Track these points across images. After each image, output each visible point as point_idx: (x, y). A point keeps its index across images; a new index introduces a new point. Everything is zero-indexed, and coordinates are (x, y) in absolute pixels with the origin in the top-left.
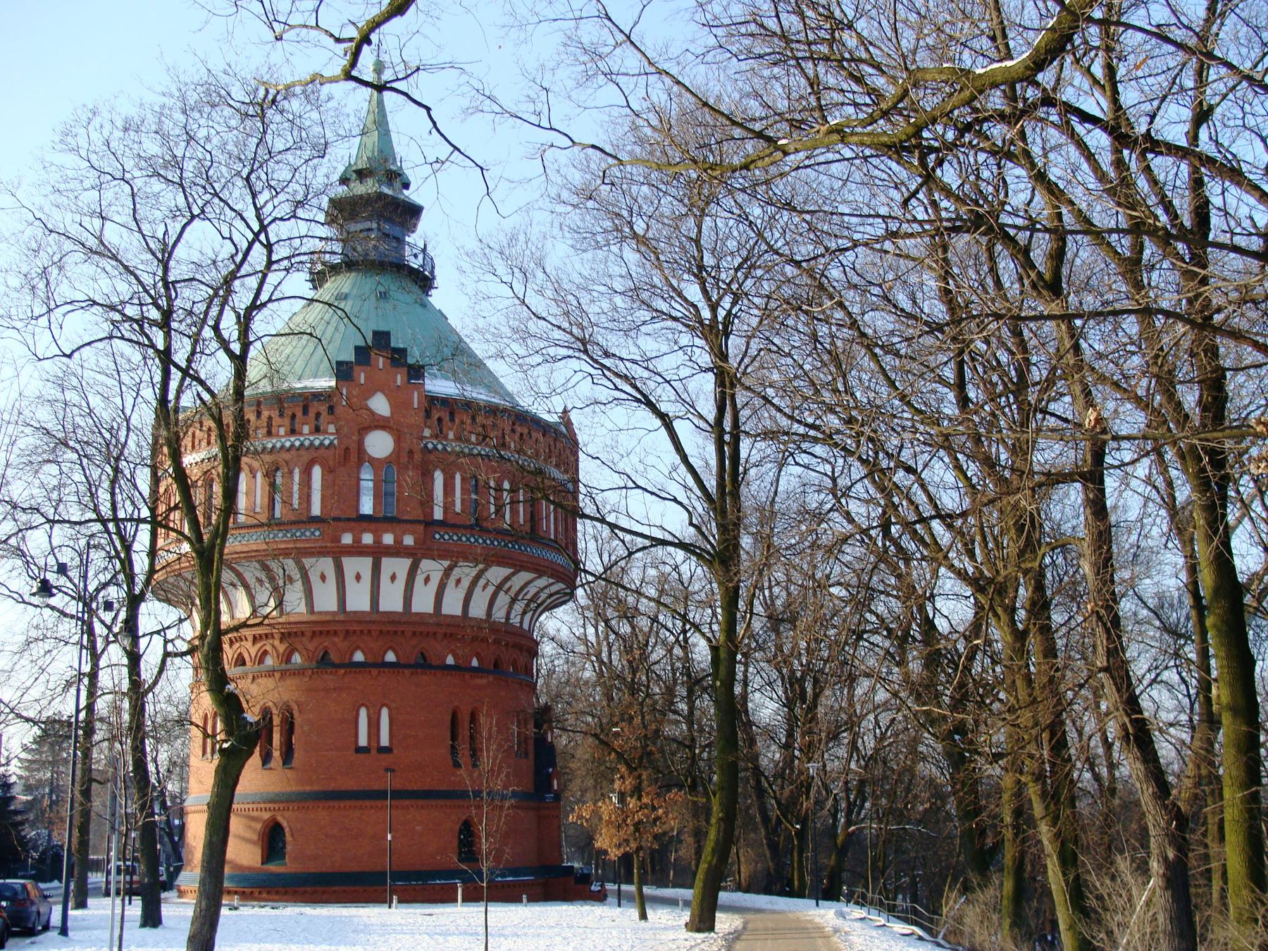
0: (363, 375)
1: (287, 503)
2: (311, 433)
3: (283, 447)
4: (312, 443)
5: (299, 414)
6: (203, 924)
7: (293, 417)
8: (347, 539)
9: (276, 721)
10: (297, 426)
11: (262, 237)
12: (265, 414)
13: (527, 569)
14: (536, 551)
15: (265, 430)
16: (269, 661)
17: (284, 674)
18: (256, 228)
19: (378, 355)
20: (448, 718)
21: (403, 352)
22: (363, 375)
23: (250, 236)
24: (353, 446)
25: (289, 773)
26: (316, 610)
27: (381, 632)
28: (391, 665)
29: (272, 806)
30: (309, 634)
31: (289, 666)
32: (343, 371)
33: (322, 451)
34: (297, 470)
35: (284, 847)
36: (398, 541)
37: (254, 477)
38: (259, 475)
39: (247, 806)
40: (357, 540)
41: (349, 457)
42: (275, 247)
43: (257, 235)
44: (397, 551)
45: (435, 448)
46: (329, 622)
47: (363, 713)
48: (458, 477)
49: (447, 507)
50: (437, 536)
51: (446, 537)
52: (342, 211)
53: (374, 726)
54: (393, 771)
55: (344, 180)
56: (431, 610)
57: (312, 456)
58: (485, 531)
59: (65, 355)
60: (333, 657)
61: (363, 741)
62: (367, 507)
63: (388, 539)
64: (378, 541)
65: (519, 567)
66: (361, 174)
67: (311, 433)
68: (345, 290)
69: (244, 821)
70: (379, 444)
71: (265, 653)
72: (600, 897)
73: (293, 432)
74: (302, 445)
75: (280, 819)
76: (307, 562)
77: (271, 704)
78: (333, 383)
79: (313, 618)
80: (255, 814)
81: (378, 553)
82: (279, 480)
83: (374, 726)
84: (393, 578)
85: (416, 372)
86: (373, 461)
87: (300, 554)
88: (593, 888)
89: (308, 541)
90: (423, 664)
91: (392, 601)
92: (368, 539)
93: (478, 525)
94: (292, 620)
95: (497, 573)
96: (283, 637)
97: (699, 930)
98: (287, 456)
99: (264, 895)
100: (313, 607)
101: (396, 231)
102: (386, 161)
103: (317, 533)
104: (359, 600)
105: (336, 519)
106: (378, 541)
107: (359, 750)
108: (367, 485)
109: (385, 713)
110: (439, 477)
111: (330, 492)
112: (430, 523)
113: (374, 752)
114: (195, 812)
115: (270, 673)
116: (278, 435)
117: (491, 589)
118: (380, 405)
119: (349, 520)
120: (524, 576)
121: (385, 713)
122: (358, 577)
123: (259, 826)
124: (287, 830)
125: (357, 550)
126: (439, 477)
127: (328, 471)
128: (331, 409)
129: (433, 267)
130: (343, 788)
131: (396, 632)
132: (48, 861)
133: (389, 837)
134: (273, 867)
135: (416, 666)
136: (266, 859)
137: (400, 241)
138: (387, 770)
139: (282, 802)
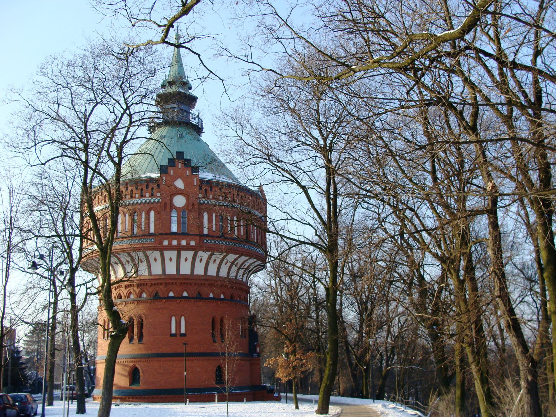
0: (172, 171)
1: (139, 227)
2: (150, 197)
3: (137, 203)
5: (144, 188)
6: (103, 413)
7: (142, 189)
8: (166, 243)
9: (135, 323)
10: (143, 194)
11: (128, 112)
12: (130, 188)
13: (245, 255)
14: (248, 247)
16: (132, 297)
17: (139, 302)
18: (125, 107)
19: (179, 162)
20: (211, 321)
21: (189, 161)
22: (172, 171)
23: (122, 111)
24: (168, 202)
25: (141, 346)
26: (152, 274)
27: (181, 283)
28: (185, 297)
29: (134, 360)
31: (141, 299)
32: (163, 169)
33: (154, 204)
34: (143, 213)
35: (139, 378)
36: (188, 243)
37: (125, 216)
38: (127, 215)
39: (123, 360)
40: (170, 243)
41: (166, 207)
42: (133, 116)
43: (125, 110)
44: (188, 248)
45: (204, 202)
46: (158, 279)
47: (173, 319)
48: (214, 215)
49: (210, 228)
50: (205, 241)
51: (209, 241)
52: (162, 99)
53: (178, 325)
54: (186, 344)
55: (163, 86)
56: (202, 273)
57: (150, 207)
58: (225, 238)
59: (42, 164)
60: (160, 294)
61: (173, 331)
62: (174, 228)
63: (184, 243)
64: (179, 243)
65: (241, 254)
66: (171, 83)
67: (150, 197)
68: (164, 134)
69: (122, 367)
70: (180, 201)
71: (130, 293)
72: (278, 399)
73: (142, 196)
75: (137, 366)
76: (149, 253)
77: (133, 315)
78: (159, 175)
79: (151, 277)
80: (126, 363)
81: (179, 249)
82: (136, 217)
83: (178, 325)
84: (186, 260)
85: (195, 169)
86: (176, 208)
87: (145, 250)
88: (275, 395)
89: (149, 243)
90: (200, 297)
91: (185, 270)
92: (175, 243)
93: (223, 236)
94: (142, 278)
95: (231, 257)
96: (138, 286)
97: (321, 413)
98: (139, 207)
99: (131, 399)
100: (151, 273)
101: (186, 108)
102: (181, 77)
103: (153, 240)
104: (171, 270)
105: (161, 234)
106: (179, 243)
107: (172, 335)
108: (174, 219)
109: (183, 319)
110: (206, 216)
111: (158, 222)
112: (202, 235)
113: (178, 336)
114: (100, 363)
115: (133, 302)
116: (135, 198)
117: (229, 264)
118: (180, 184)
119: (166, 234)
120: (244, 258)
121: (183, 319)
122: (171, 259)
123: (128, 369)
124: (140, 371)
125: (170, 247)
126: (206, 216)
127: (157, 213)
128: (158, 186)
129: (202, 124)
130: (165, 352)
131: (187, 283)
132: (36, 385)
133: (185, 374)
134: (134, 387)
135: (197, 298)
136: (131, 384)
137: (188, 113)
138: (184, 344)
139: (137, 358)
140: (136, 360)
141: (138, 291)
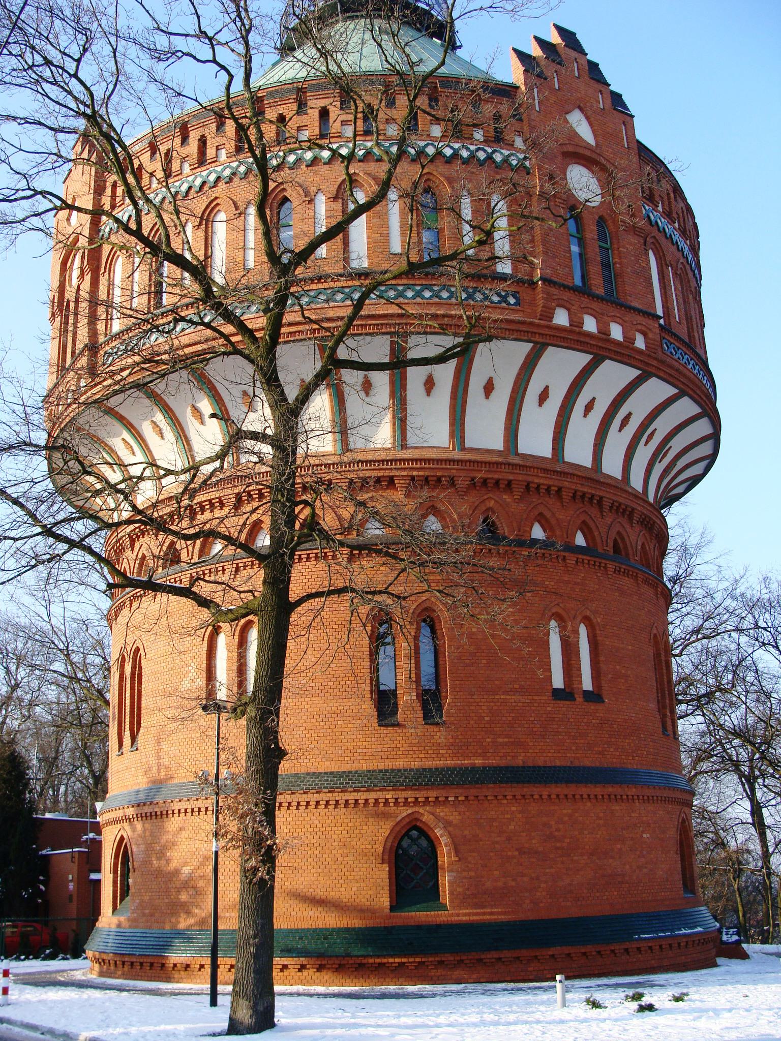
2: (486, 141)
3: (439, 153)
4: (490, 158)
8: (561, 318)
25: (440, 735)
26: (467, 446)
30: (461, 483)
36: (629, 340)
40: (577, 323)
44: (623, 353)
60: (504, 529)
67: (486, 141)
74: (472, 156)
75: (427, 818)
79: (468, 456)
81: (600, 350)
107: (557, 693)
113: (579, 699)
121: (583, 631)
124: (444, 840)
130: (540, 762)
140: (421, 795)
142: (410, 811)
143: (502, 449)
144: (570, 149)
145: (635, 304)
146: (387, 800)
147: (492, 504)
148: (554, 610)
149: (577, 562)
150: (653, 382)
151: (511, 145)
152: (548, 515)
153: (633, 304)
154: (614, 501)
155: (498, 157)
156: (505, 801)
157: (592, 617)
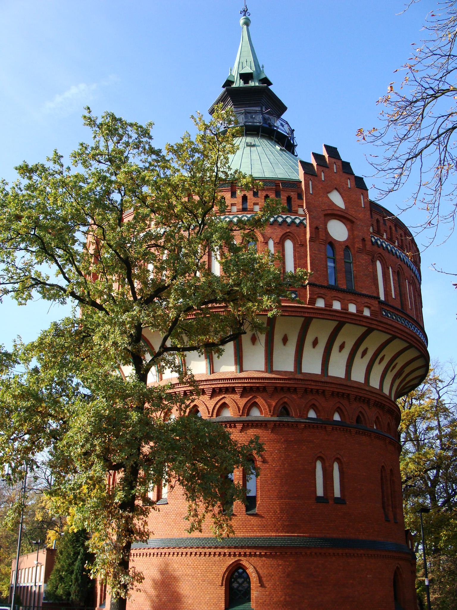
4: (284, 221)
8: (320, 303)
15: (241, 207)
25: (254, 520)
26: (274, 369)
29: (237, 551)
34: (271, 243)
40: (329, 305)
47: (319, 466)
61: (320, 492)
63: (352, 308)
66: (246, 77)
71: (224, 406)
96: (245, 391)
100: (272, 366)
106: (345, 308)
107: (319, 499)
109: (336, 466)
113: (331, 502)
119: (322, 287)
121: (336, 466)
140: (242, 551)
141: (242, 402)
142: (236, 559)
143: (293, 371)
144: (329, 212)
145: (364, 292)
146: (225, 553)
147: (286, 400)
148: (319, 455)
149: (333, 429)
150: (375, 334)
151: (296, 213)
152: (317, 404)
153: (363, 292)
154: (357, 396)
155: (289, 220)
156: (286, 556)
157: (341, 458)
